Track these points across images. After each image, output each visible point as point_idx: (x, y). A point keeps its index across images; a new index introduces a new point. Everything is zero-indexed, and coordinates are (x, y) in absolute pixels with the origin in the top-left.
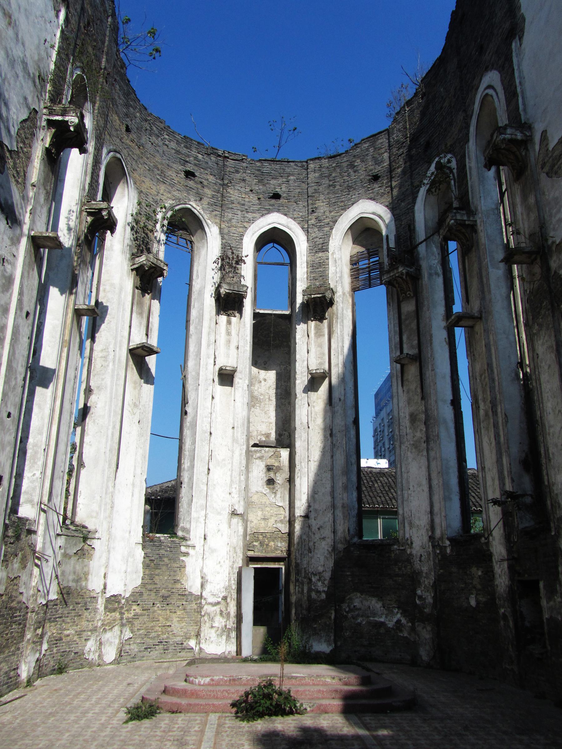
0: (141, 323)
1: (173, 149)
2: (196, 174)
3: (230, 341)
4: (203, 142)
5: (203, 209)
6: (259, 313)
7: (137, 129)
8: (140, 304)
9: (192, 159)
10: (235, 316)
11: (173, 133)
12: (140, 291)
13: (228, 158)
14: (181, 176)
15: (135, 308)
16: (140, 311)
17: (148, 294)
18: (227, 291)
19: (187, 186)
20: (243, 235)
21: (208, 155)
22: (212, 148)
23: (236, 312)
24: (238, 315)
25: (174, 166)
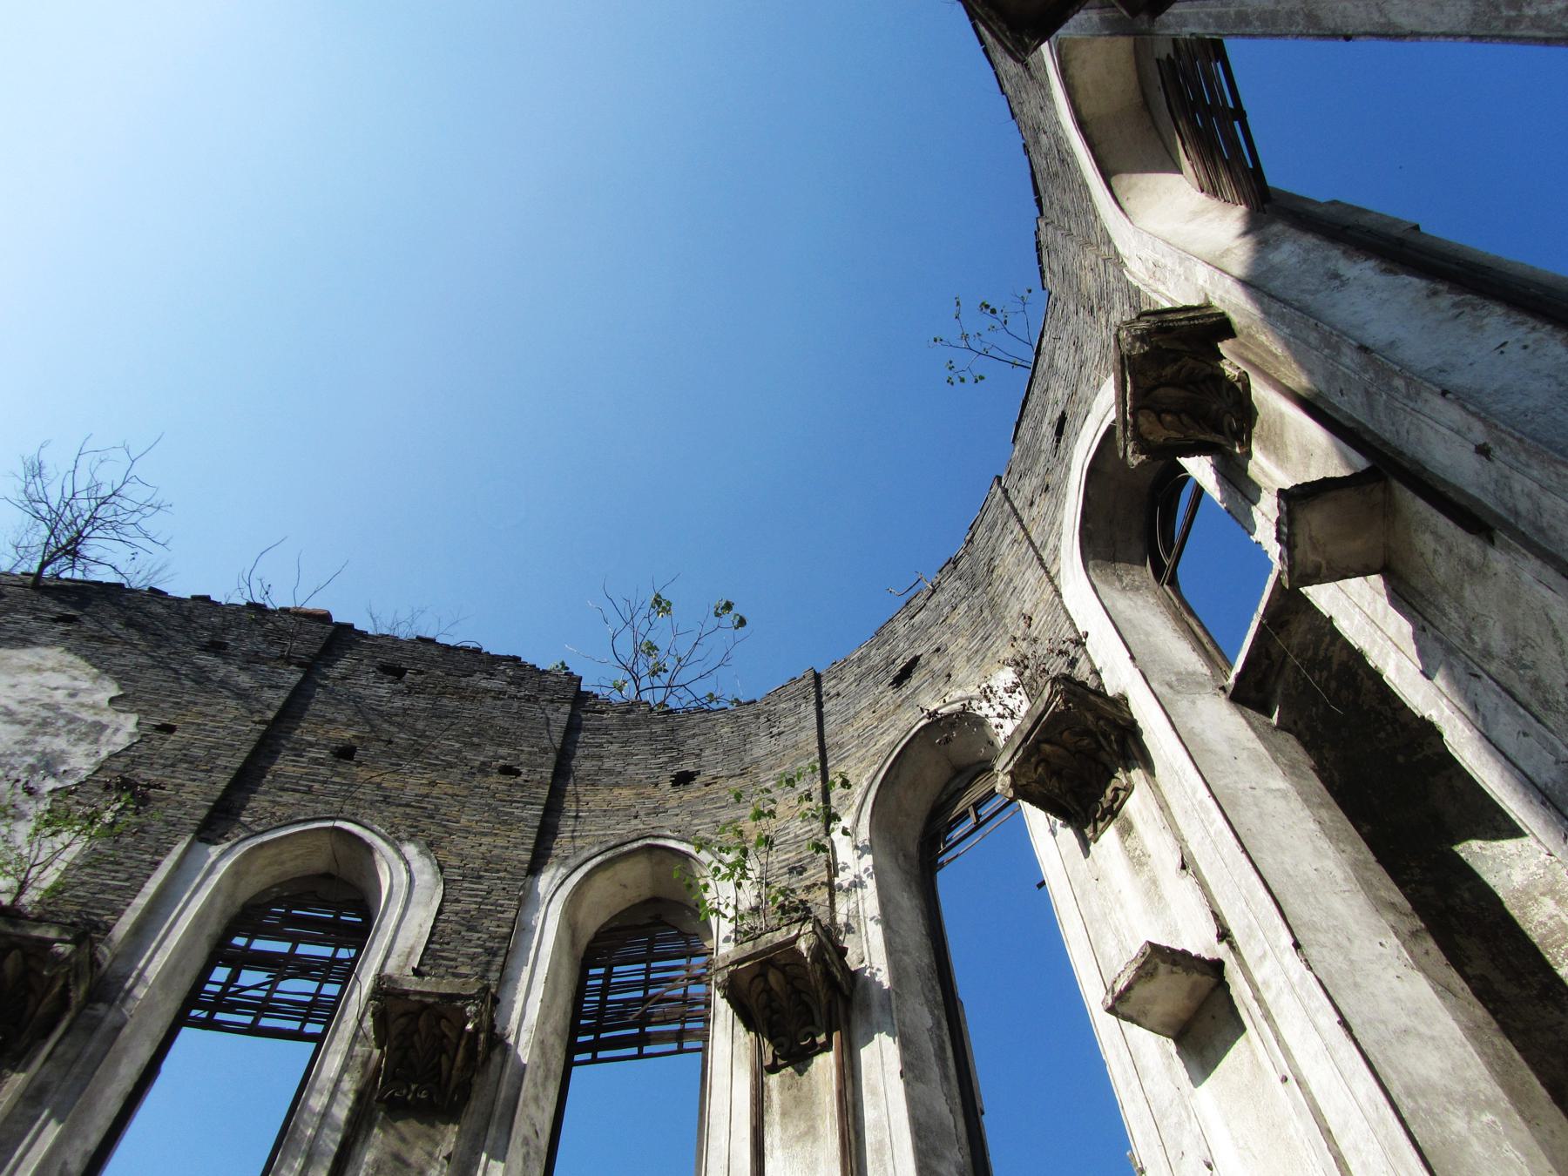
0: (812, 1166)
1: (851, 684)
2: (919, 654)
3: (1154, 882)
4: (911, 593)
5: (960, 686)
6: (1239, 677)
7: (724, 753)
8: (801, 1104)
9: (902, 645)
10: (1129, 789)
11: (845, 661)
12: (790, 1069)
13: (974, 535)
14: (884, 701)
15: (772, 1138)
16: (803, 1127)
17: (826, 1047)
18: (1010, 767)
19: (907, 697)
20: (1060, 596)
21: (934, 591)
22: (940, 571)
23: (1120, 774)
24: (1137, 775)
25: (864, 703)
